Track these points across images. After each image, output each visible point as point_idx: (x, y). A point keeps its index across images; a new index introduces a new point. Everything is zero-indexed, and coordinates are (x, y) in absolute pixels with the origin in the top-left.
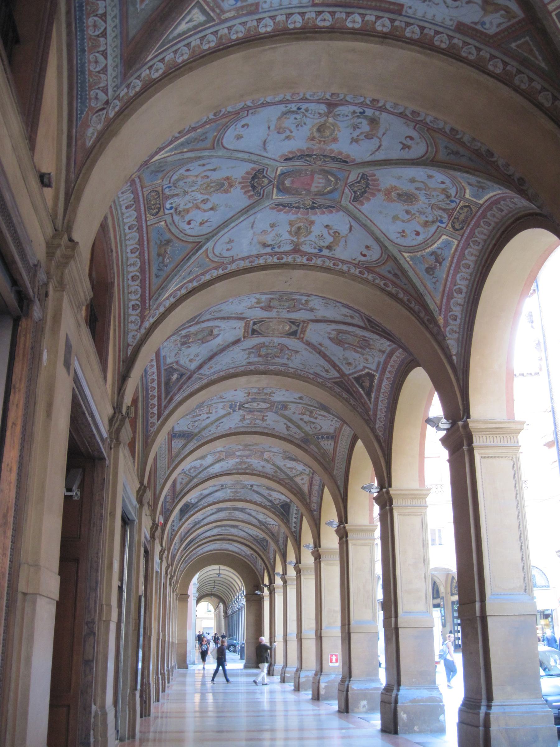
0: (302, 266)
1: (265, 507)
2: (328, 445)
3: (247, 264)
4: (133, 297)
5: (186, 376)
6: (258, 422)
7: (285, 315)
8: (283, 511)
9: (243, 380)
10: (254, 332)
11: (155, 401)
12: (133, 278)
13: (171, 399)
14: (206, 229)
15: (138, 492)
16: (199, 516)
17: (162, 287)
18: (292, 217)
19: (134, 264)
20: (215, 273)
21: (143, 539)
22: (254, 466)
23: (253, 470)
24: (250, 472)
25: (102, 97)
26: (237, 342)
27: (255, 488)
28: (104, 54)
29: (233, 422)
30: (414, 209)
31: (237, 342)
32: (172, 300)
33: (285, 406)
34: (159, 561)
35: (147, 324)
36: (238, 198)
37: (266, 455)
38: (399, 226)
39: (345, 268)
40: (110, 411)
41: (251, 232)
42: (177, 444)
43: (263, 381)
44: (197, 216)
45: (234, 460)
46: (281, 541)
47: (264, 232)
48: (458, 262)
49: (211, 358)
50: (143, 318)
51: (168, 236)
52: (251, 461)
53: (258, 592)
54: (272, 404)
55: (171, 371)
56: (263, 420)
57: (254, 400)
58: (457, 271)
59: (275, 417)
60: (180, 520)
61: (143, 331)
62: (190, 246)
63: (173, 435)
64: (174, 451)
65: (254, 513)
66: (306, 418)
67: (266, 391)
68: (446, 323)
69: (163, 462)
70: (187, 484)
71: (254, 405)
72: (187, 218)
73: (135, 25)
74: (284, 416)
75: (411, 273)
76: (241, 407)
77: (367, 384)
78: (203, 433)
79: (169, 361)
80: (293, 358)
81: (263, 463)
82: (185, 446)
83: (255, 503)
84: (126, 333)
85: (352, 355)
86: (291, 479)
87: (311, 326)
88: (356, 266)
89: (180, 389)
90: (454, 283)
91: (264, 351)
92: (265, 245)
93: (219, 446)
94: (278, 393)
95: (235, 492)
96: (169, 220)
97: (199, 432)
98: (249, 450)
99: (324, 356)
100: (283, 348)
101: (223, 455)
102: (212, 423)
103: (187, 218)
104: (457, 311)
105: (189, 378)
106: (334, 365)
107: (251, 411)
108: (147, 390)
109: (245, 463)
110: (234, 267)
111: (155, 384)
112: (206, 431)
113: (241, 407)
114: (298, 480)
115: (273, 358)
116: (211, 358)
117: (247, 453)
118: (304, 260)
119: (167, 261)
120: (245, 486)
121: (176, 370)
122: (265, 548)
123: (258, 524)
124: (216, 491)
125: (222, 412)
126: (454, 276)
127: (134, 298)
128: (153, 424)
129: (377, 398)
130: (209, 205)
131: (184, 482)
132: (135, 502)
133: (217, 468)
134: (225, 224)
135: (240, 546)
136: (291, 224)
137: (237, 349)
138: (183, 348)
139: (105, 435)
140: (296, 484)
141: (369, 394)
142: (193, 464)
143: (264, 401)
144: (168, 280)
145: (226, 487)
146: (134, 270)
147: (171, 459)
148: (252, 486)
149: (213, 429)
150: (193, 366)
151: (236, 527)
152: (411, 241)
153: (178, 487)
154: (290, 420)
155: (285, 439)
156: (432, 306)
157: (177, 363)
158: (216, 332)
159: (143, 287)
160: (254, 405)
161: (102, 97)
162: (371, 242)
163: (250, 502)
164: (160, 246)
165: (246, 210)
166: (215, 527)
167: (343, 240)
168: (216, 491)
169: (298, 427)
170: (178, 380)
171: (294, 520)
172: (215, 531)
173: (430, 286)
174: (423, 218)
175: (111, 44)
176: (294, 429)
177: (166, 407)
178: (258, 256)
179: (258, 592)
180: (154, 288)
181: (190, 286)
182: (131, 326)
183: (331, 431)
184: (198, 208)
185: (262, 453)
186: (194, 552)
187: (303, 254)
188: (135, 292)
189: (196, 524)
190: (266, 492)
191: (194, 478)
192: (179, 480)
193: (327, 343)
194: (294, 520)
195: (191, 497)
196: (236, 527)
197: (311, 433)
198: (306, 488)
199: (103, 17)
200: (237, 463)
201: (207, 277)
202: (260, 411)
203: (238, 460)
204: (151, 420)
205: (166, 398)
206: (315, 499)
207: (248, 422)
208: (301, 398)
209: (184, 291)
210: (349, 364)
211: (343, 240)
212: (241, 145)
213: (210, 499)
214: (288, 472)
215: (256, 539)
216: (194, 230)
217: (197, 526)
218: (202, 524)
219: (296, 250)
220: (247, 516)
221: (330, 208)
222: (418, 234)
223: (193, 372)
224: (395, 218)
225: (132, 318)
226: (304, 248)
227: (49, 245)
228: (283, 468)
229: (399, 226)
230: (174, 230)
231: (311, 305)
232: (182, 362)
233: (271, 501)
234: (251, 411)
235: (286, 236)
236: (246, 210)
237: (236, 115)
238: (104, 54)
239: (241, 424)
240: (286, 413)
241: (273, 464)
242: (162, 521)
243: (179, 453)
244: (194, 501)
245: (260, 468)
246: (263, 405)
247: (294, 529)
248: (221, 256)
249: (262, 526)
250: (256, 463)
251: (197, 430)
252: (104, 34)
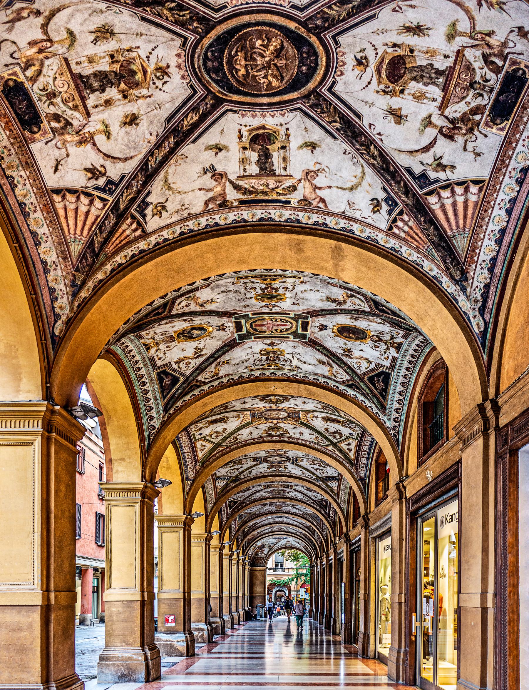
7: (276, 489)
45: (288, 406)
52: (264, 405)
57: (280, 462)
67: (274, 469)
71: (279, 459)
94: (265, 469)
98: (272, 419)
113: (289, 459)
143: (273, 462)
145: (296, 318)
160: (279, 459)
200: (283, 402)
202: (273, 456)
203: (282, 405)
208: (250, 472)
234: (280, 456)
246: (271, 459)
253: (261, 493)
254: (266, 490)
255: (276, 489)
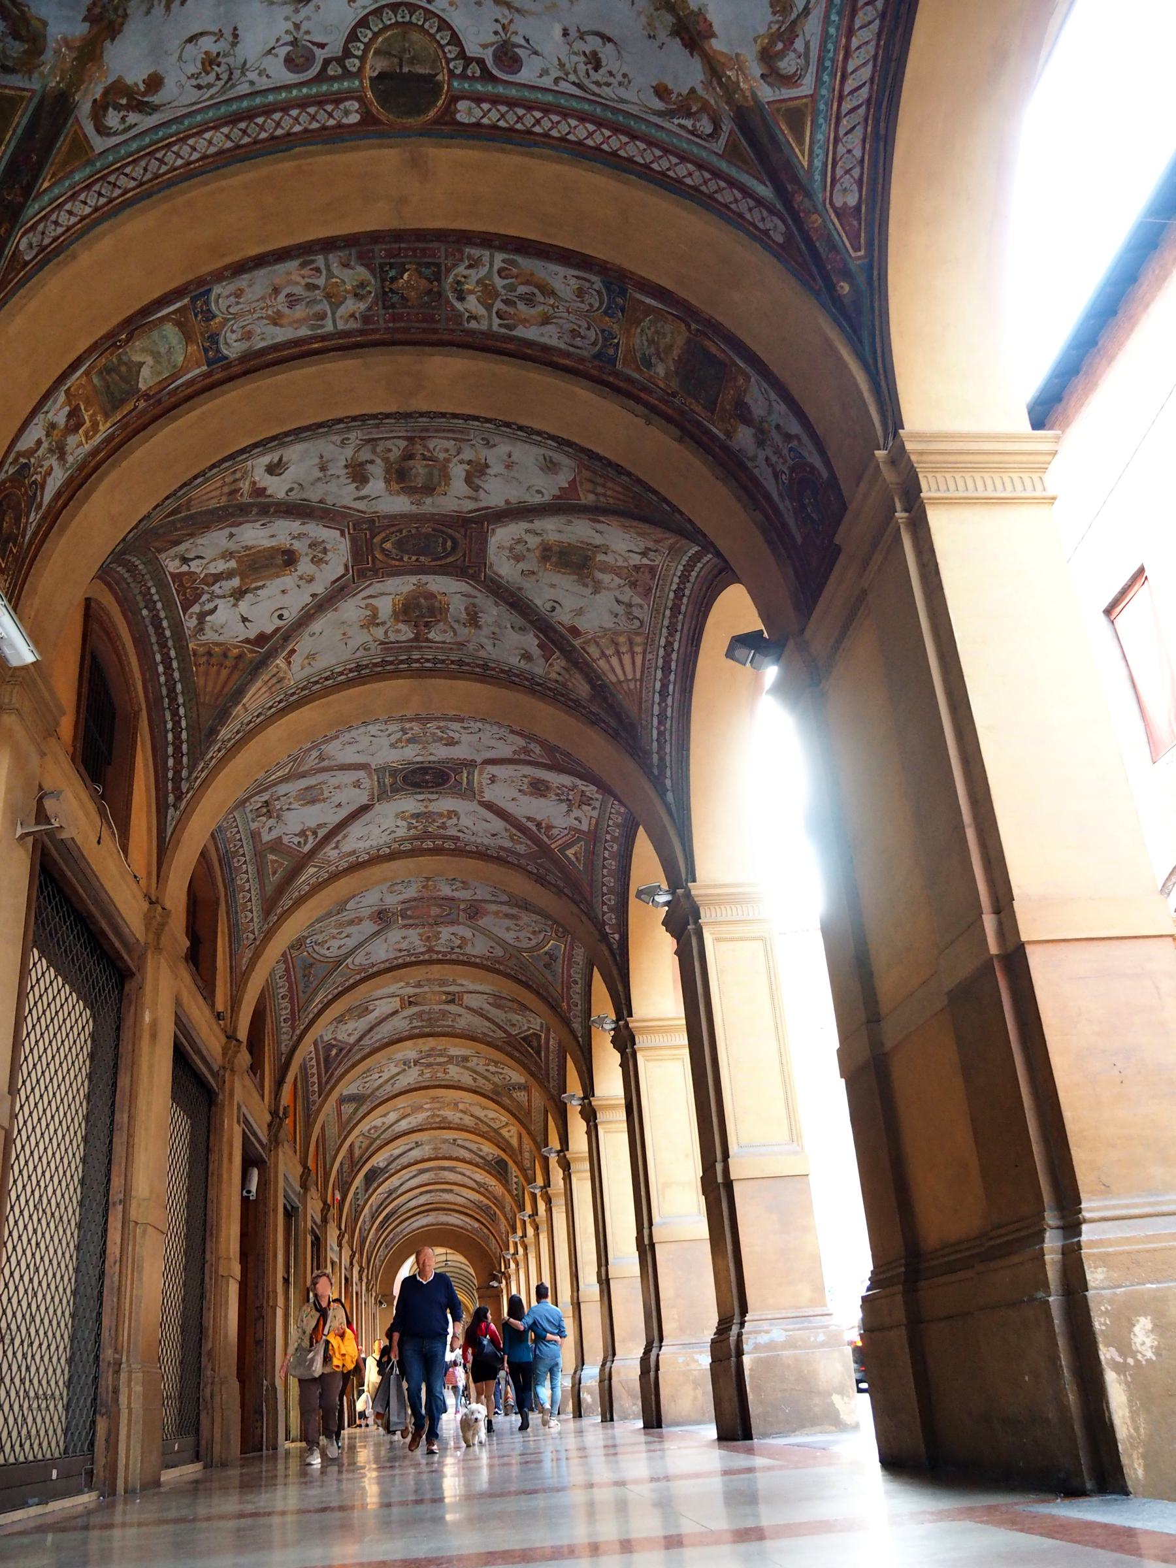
0: (439, 962)
1: (477, 1165)
2: (521, 1096)
3: (387, 965)
4: (284, 1012)
5: (345, 1050)
6: (439, 1075)
7: (437, 989)
8: (499, 1169)
9: (409, 1043)
10: (410, 1003)
11: (315, 1079)
12: (283, 998)
13: (332, 1074)
14: (344, 951)
15: (301, 1177)
16: (394, 1181)
17: (309, 1001)
18: (419, 930)
19: (283, 986)
20: (358, 977)
21: (309, 1224)
22: (450, 1118)
23: (450, 1123)
24: (446, 1126)
25: (251, 936)
26: (395, 1013)
27: (459, 1142)
28: (251, 911)
29: (411, 1077)
30: (521, 923)
31: (395, 1013)
32: (320, 1006)
33: (465, 1059)
34: (336, 1248)
35: (298, 1032)
36: (369, 927)
37: (461, 1106)
38: (513, 934)
39: (478, 960)
40: (268, 1118)
41: (385, 946)
42: (347, 1109)
43: (431, 1042)
44: (335, 943)
46: (508, 1208)
47: (398, 942)
48: (569, 960)
49: (371, 1029)
50: (293, 1029)
51: (311, 961)
53: (495, 1284)
54: (451, 1058)
55: (329, 1047)
56: (445, 1073)
57: (429, 1056)
58: (570, 967)
59: (458, 1069)
60: (366, 1191)
61: (295, 1038)
62: (331, 965)
63: (342, 1100)
64: (345, 1117)
65: (467, 1173)
66: (492, 1069)
68: (570, 1009)
69: (332, 1131)
70: (367, 1149)
71: (431, 1060)
72: (326, 946)
73: (269, 889)
74: (467, 1068)
75: (532, 968)
76: (416, 1063)
77: (535, 1044)
78: (377, 1093)
79: (326, 1039)
80: (458, 1019)
81: (459, 1115)
82: (356, 1110)
83: (464, 1161)
84: (279, 1043)
85: (516, 1018)
86: (496, 1131)
87: (465, 996)
88: (488, 959)
89: (340, 1063)
90: (570, 976)
91: (425, 1017)
92: (400, 951)
93: (401, 1102)
95: (434, 1149)
96: (310, 950)
97: (372, 1093)
99: (488, 1019)
100: (444, 1013)
101: (408, 1110)
102: (387, 1082)
103: (326, 946)
104: (577, 998)
105: (350, 1051)
106: (500, 1027)
107: (429, 1065)
108: (306, 1069)
109: (438, 1116)
110: (375, 969)
111: (314, 1062)
112: (381, 1090)
113: (416, 1063)
114: (504, 1132)
115: (437, 1021)
116: (371, 1029)
117: (437, 1105)
118: (440, 956)
119: (311, 979)
120: (446, 1141)
121: (334, 1046)
122: (493, 1218)
123: (475, 1186)
124: (410, 1150)
125: (397, 1070)
126: (568, 971)
127: (285, 1013)
128: (314, 1102)
129: (547, 1057)
130: (344, 935)
131: (364, 1146)
132: (298, 1189)
133: (404, 1125)
134: (361, 945)
135: (462, 1217)
136: (420, 935)
137: (396, 1018)
138: (340, 1025)
139: (265, 1140)
140: (503, 1138)
141: (539, 1054)
142: (373, 1124)
143: (441, 1055)
144: (315, 992)
146: (283, 991)
147: (342, 1127)
148: (455, 1140)
149: (388, 1087)
150: (352, 1040)
151: (451, 1191)
152: (525, 944)
153: (357, 1152)
154: (475, 1072)
155: (475, 1092)
156: (555, 995)
157: (335, 1039)
158: (371, 1008)
159: (291, 1002)
160: (431, 1060)
161: (251, 936)
162: (493, 944)
163: (457, 1159)
164: (305, 968)
165: (376, 934)
166: (421, 1194)
167: (470, 944)
168: (410, 1150)
169: (485, 1078)
170: (337, 1055)
171: (515, 1180)
172: (422, 1200)
173: (550, 978)
174: (531, 929)
175: (255, 905)
176: (481, 1081)
177: (327, 1083)
178: (396, 958)
179: (495, 1284)
180: (302, 1002)
181: (336, 991)
182: (284, 1037)
183: (522, 1080)
184: (334, 938)
185: (456, 1104)
186: (398, 1229)
187: (438, 952)
188: (286, 1008)
189: (390, 1193)
190: (474, 1147)
191: (375, 1140)
192: (357, 1144)
193: (487, 1007)
194: (515, 1180)
195: (379, 1160)
196: (451, 1191)
197: (500, 1083)
198: (514, 1142)
199: (249, 891)
201: (351, 981)
202: (439, 1064)
203: (428, 1113)
204: (312, 1098)
205: (326, 1072)
206: (527, 1155)
207: (428, 1075)
209: (330, 997)
210: (514, 1025)
211: (470, 944)
212: (361, 905)
213: (404, 1160)
214: (492, 1124)
215: (479, 1206)
216: (334, 952)
217: (394, 1196)
218: (399, 1192)
219: (430, 950)
220: (460, 1176)
221: (453, 923)
222: (530, 939)
223: (354, 1045)
224: (508, 929)
225: (284, 1030)
226: (436, 949)
227: (223, 1048)
228: (485, 1119)
229: (513, 934)
230: (315, 955)
231: (459, 982)
232: (340, 1038)
233: (482, 1157)
234: (429, 1065)
235: (418, 942)
236: (376, 934)
237: (354, 896)
238: (251, 911)
239: (420, 1079)
240: (468, 1065)
241: (472, 1115)
242: (338, 1196)
243: (350, 1119)
244: (382, 1165)
245: (458, 1121)
247: (515, 1192)
248: (361, 965)
249: (481, 1188)
250: (453, 1116)
251: (369, 1091)
252: (250, 900)
253: (471, 987)
254: (459, 989)
255: (437, 989)
